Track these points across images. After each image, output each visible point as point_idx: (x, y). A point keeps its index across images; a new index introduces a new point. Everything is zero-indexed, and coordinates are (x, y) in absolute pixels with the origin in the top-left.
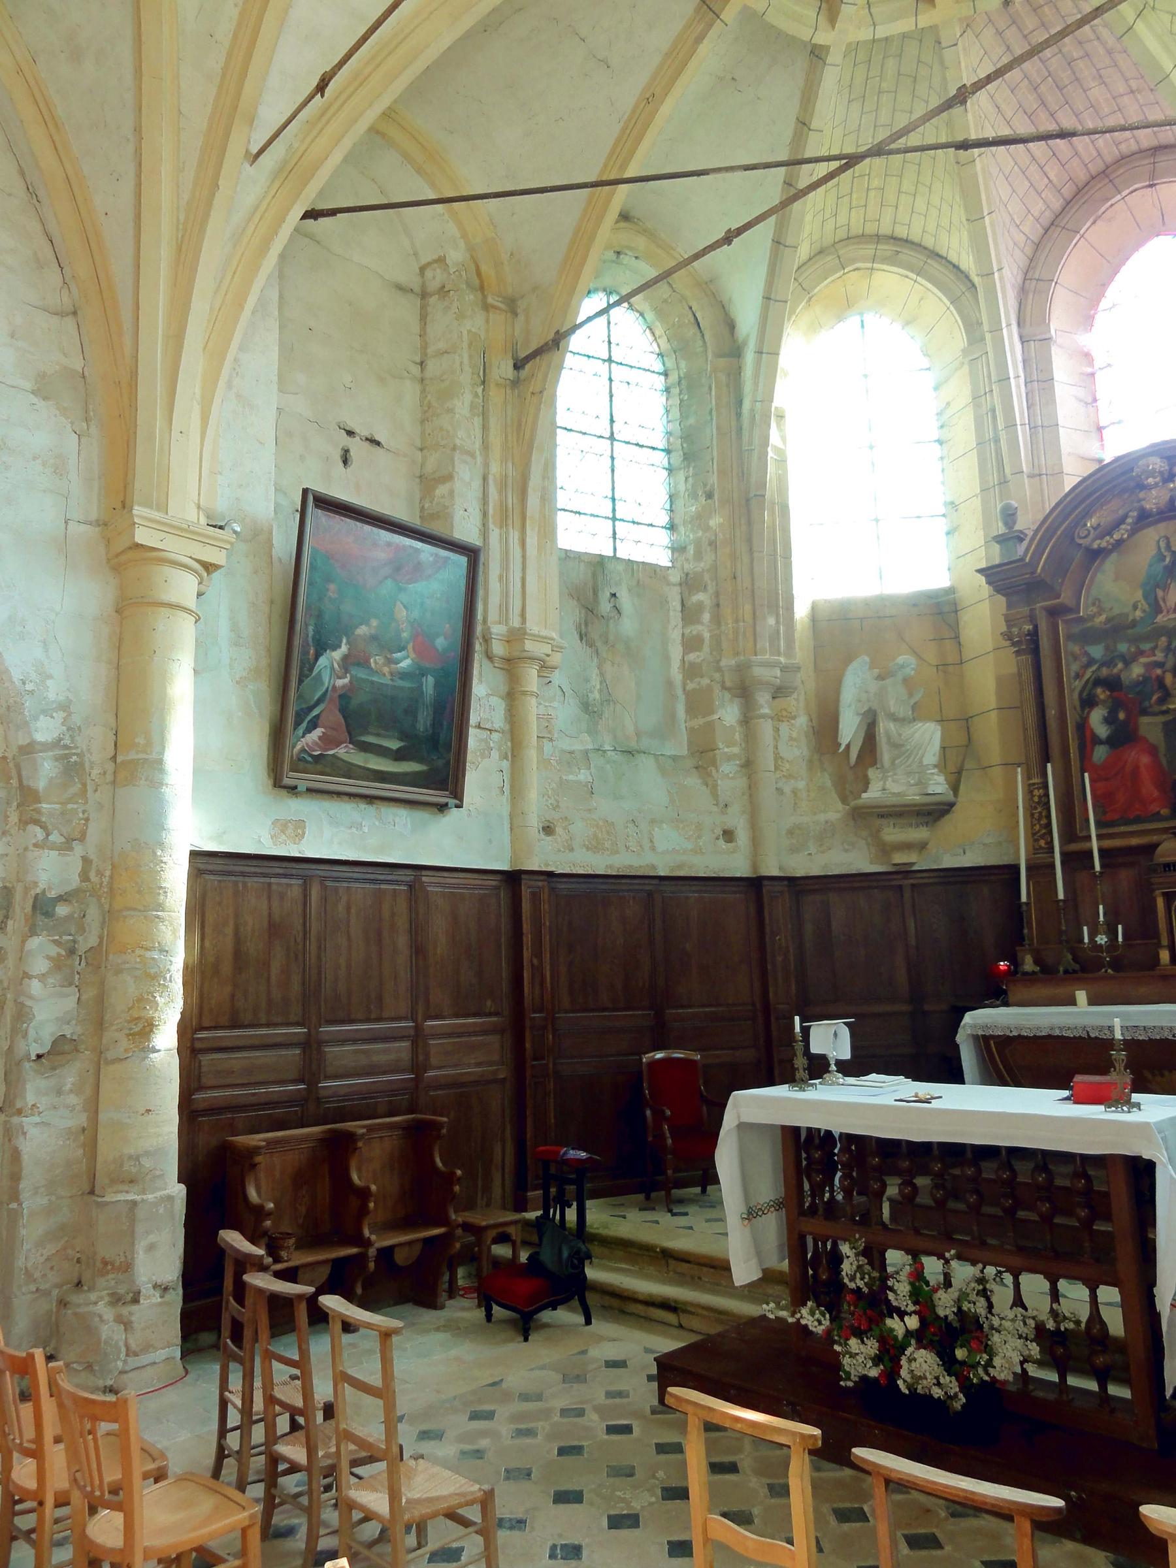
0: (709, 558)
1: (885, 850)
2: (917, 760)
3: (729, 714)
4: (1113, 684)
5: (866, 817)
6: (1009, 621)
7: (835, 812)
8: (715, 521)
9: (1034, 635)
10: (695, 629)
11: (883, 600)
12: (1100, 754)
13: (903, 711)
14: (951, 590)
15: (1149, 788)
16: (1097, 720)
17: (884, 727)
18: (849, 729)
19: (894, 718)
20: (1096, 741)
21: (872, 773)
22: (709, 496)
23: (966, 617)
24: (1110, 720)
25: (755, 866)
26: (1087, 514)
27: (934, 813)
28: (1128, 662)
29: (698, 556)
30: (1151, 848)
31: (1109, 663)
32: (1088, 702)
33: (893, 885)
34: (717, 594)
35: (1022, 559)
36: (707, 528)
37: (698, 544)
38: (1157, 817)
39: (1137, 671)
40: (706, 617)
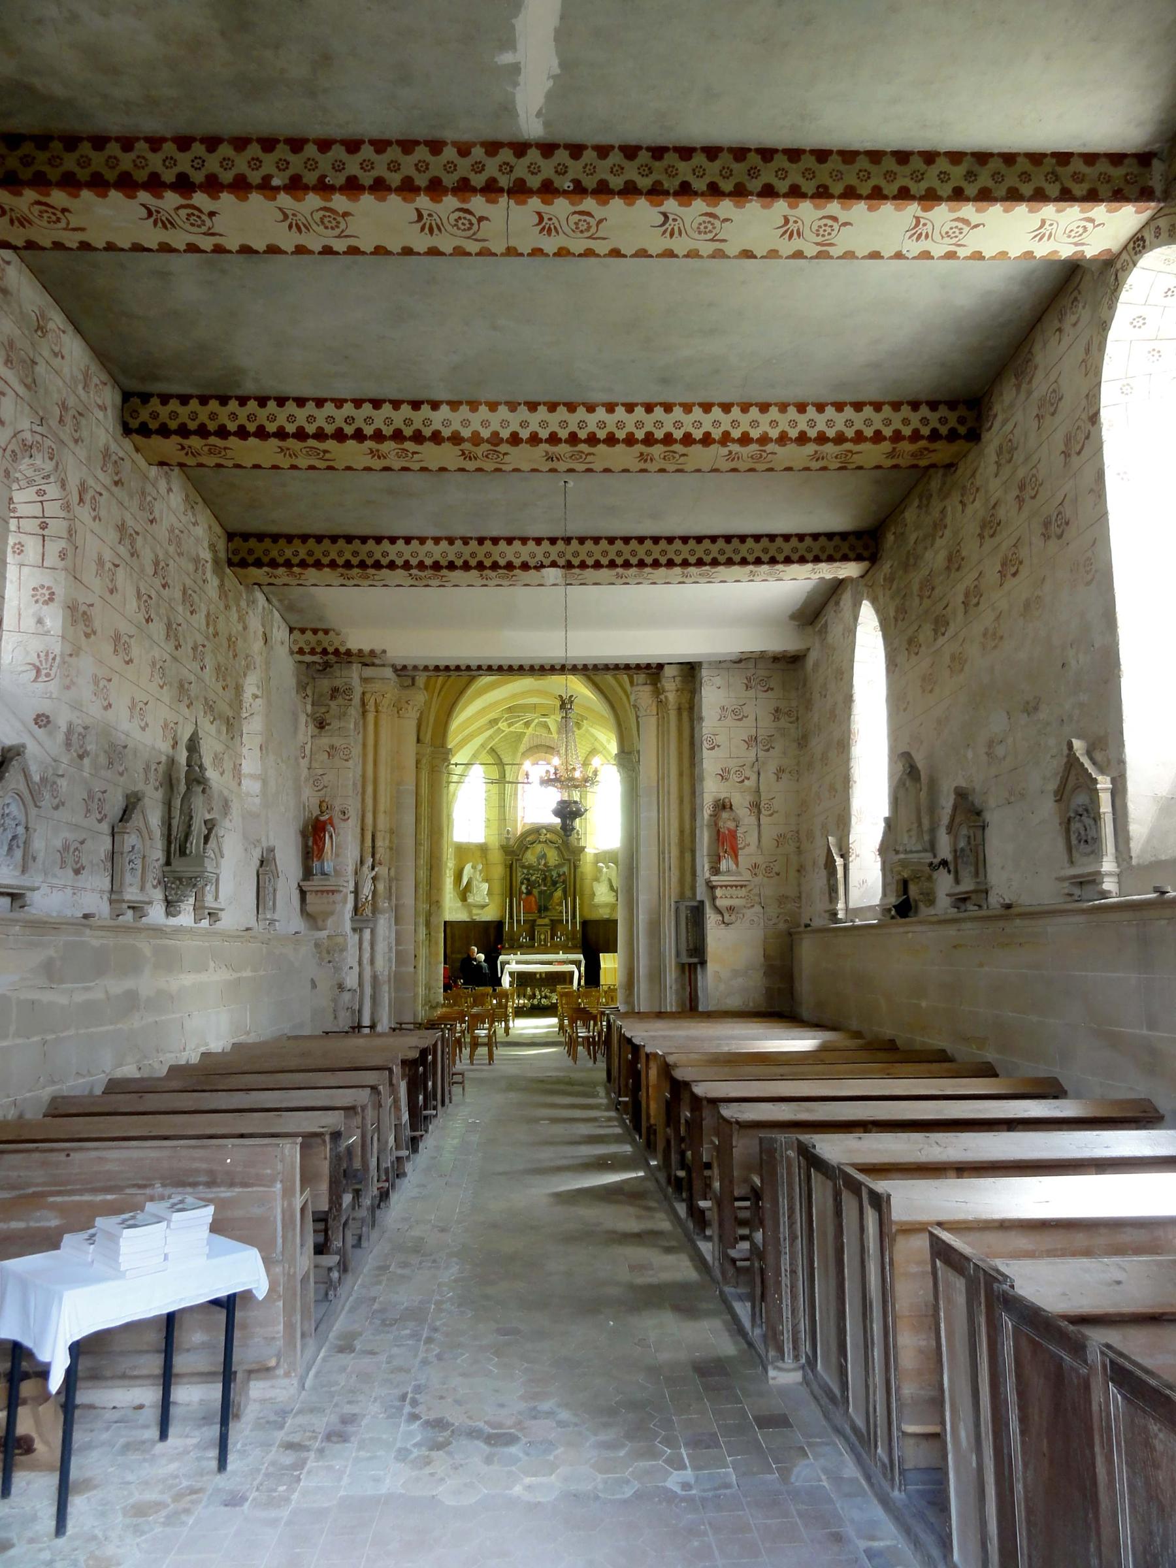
1: (470, 912)
2: (481, 892)
4: (528, 880)
5: (469, 907)
7: (460, 904)
12: (524, 896)
14: (485, 844)
15: (534, 906)
16: (524, 887)
17: (475, 883)
27: (483, 907)
30: (535, 921)
32: (522, 883)
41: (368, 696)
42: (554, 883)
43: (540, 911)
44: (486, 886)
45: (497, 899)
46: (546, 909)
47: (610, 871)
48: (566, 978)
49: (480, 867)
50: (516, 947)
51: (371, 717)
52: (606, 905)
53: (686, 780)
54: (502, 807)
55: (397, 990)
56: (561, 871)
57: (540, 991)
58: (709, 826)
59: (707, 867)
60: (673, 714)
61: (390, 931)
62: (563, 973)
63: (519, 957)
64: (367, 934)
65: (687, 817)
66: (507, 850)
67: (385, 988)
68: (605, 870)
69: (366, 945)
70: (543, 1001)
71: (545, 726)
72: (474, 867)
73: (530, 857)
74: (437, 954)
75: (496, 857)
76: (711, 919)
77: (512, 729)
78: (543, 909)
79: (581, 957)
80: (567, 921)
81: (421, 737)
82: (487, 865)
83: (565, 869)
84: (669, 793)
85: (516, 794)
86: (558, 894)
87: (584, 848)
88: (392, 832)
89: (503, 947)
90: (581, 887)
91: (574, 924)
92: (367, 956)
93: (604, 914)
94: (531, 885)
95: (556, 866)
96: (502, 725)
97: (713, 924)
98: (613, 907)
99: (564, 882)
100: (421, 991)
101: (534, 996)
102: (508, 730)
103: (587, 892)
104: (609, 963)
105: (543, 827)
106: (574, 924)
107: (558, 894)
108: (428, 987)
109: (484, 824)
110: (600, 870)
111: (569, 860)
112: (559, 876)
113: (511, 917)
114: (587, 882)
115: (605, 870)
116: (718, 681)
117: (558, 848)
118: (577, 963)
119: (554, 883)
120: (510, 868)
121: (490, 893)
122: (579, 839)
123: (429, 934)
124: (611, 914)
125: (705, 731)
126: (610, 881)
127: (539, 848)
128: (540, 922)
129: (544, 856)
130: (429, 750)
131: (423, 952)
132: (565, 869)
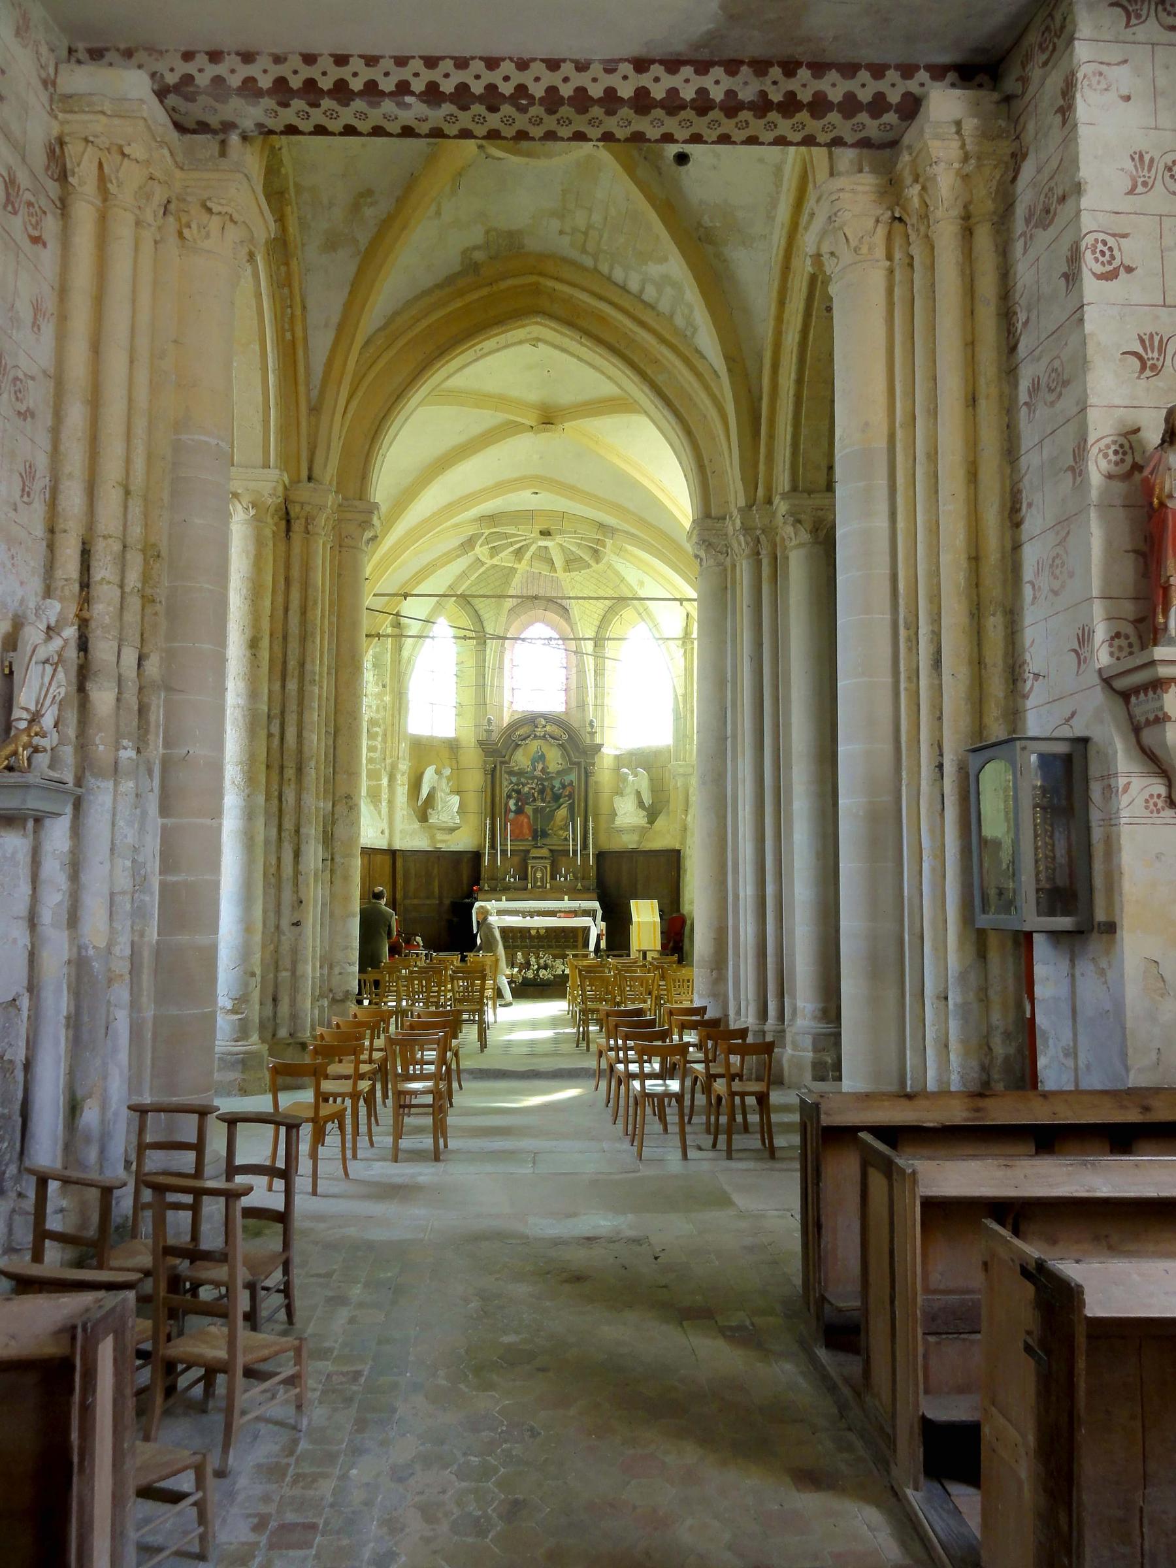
0: (382, 713)
2: (448, 808)
3: (385, 781)
4: (518, 792)
5: (431, 830)
6: (485, 762)
7: (417, 825)
8: (387, 698)
9: (494, 770)
10: (374, 743)
11: (431, 738)
12: (511, 816)
13: (448, 790)
14: (456, 740)
15: (526, 830)
16: (511, 803)
17: (439, 795)
18: (425, 791)
19: (442, 791)
20: (510, 811)
21: (430, 811)
22: (384, 686)
23: (461, 751)
24: (516, 804)
25: (390, 844)
26: (517, 729)
27: (452, 830)
28: (524, 786)
29: (377, 711)
30: (528, 851)
31: (518, 785)
32: (509, 797)
33: (436, 856)
34: (385, 730)
35: (497, 744)
36: (382, 701)
37: (378, 707)
38: (527, 840)
39: (526, 789)
40: (380, 739)
41: (73, 149)
42: (556, 798)
43: (535, 838)
44: (455, 800)
45: (473, 820)
46: (544, 834)
47: (640, 781)
48: (576, 937)
49: (447, 772)
50: (499, 889)
51: (84, 212)
52: (633, 829)
53: (988, 410)
54: (481, 686)
55: (162, 996)
56: (567, 779)
57: (538, 957)
58: (1105, 507)
59: (1101, 633)
60: (946, 233)
61: (142, 830)
62: (574, 930)
63: (504, 904)
64: (58, 836)
65: (992, 516)
66: (487, 747)
67: (121, 993)
68: (631, 778)
69: (54, 870)
70: (542, 973)
71: (545, 557)
72: (438, 772)
73: (521, 760)
74: (347, 899)
75: (472, 758)
76: (1132, 793)
77: (496, 561)
78: (539, 834)
79: (596, 905)
80: (575, 852)
81: (317, 471)
82: (458, 769)
83: (573, 777)
84: (933, 456)
85: (501, 668)
86: (563, 812)
87: (600, 746)
88: (151, 553)
89: (480, 890)
90: (596, 806)
91: (585, 857)
92: (54, 899)
93: (629, 841)
94: (522, 799)
95: (558, 773)
96: (481, 551)
97: (1138, 808)
98: (643, 832)
99: (570, 796)
100: (310, 970)
101: (528, 965)
102: (489, 562)
103: (604, 809)
104: (645, 916)
105: (542, 715)
106: (585, 857)
107: (563, 812)
108: (328, 962)
109: (454, 711)
110: (623, 779)
111: (579, 764)
112: (564, 787)
113: (493, 846)
114: (604, 797)
115: (631, 778)
116: (1123, 78)
117: (562, 746)
118: (591, 913)
119: (556, 798)
120: (492, 774)
121: (462, 810)
122: (593, 734)
123: (330, 859)
124: (640, 842)
125: (1087, 222)
126: (638, 793)
127: (534, 746)
128: (535, 853)
129: (542, 758)
130: (331, 500)
131: (315, 893)
132: (573, 777)
